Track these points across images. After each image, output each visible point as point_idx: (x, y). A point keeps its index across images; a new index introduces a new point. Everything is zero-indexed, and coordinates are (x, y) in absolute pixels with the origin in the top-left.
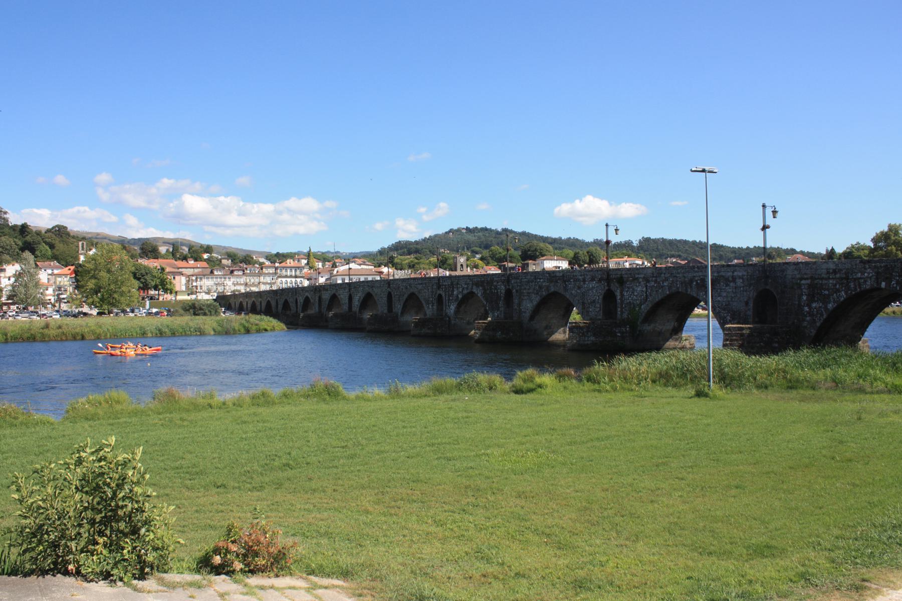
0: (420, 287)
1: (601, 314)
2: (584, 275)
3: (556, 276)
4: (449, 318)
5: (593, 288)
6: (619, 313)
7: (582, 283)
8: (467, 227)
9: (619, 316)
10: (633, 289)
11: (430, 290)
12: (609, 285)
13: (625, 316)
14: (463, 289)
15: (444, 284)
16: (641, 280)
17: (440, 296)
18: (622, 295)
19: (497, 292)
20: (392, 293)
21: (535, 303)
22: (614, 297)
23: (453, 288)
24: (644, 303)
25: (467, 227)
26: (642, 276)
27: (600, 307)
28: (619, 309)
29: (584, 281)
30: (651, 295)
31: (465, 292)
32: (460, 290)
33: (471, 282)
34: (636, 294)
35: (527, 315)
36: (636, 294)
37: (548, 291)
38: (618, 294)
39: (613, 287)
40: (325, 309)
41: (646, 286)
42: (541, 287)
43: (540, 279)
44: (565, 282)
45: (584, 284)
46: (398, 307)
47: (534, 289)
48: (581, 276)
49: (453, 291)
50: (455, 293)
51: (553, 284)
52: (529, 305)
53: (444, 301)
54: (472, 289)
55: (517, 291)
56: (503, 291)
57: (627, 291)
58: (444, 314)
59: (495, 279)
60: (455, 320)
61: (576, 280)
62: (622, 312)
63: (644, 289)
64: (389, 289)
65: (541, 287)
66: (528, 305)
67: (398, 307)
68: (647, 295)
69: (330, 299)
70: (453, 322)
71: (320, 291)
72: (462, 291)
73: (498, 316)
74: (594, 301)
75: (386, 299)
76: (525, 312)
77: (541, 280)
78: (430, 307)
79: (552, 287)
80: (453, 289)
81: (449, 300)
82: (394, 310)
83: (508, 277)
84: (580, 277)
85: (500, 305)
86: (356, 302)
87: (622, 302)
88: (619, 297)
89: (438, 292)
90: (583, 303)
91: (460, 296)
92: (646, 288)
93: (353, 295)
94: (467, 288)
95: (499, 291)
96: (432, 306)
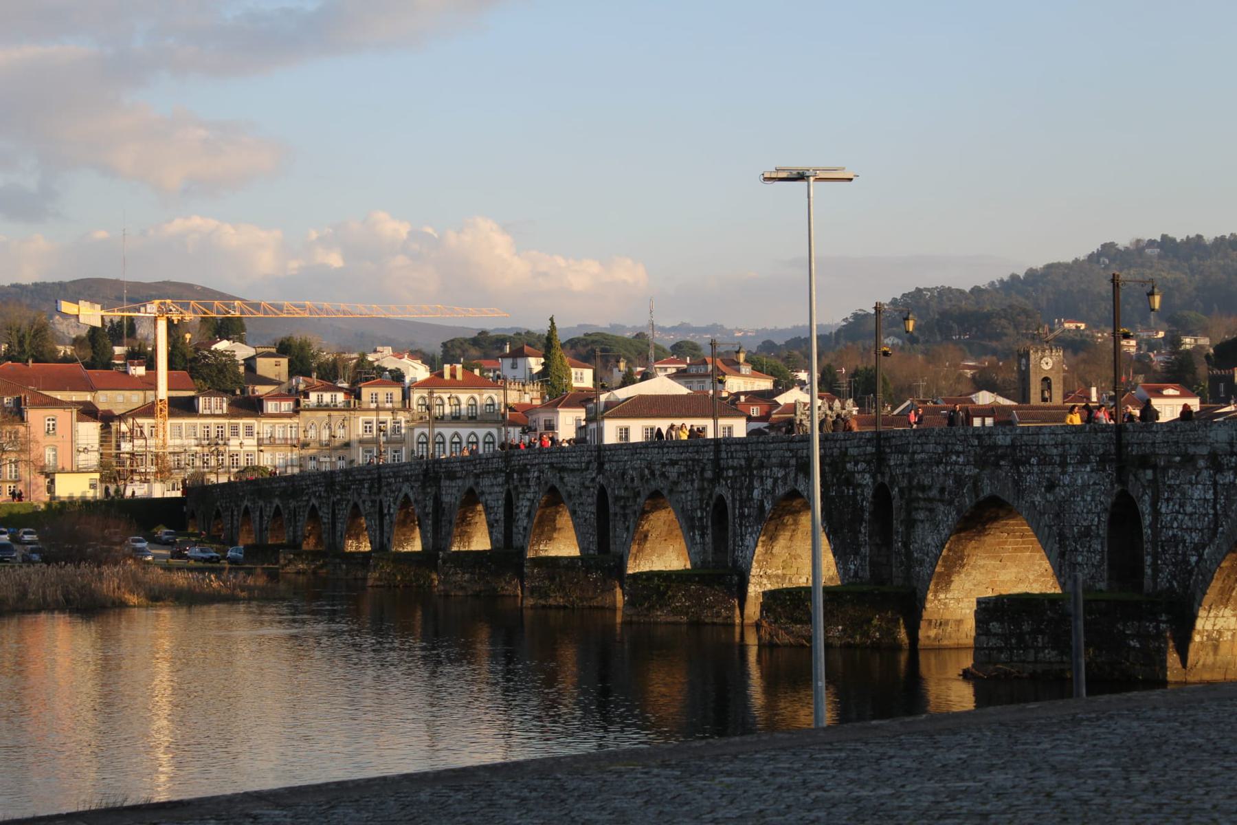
1: (1106, 575)
2: (1063, 444)
3: (995, 447)
5: (1085, 486)
6: (1149, 571)
7: (1059, 470)
8: (1164, 237)
9: (1147, 583)
10: (1184, 494)
12: (1121, 479)
13: (1163, 584)
14: (776, 480)
16: (1201, 463)
17: (721, 499)
18: (1156, 513)
19: (855, 494)
20: (609, 491)
22: (1136, 517)
23: (752, 476)
24: (1211, 540)
25: (1164, 237)
26: (1205, 451)
27: (1103, 551)
28: (1148, 560)
29: (1063, 464)
30: (1227, 516)
33: (793, 462)
34: (1189, 509)
36: (1189, 509)
37: (977, 496)
38: (1145, 507)
39: (1134, 490)
41: (1215, 484)
42: (959, 481)
43: (958, 454)
44: (1016, 463)
45: (1064, 473)
47: (942, 490)
48: (1056, 446)
49: (751, 489)
50: (756, 493)
51: (987, 471)
52: (929, 540)
53: (730, 517)
54: (796, 481)
55: (901, 491)
56: (869, 492)
57: (1168, 500)
58: (730, 565)
59: (852, 451)
61: (1044, 461)
62: (1156, 570)
63: (1210, 495)
64: (600, 479)
65: (959, 481)
68: (1216, 514)
71: (437, 480)
72: (774, 489)
73: (856, 573)
74: (1087, 533)
77: (961, 460)
78: (698, 537)
79: (986, 481)
80: (751, 482)
81: (742, 515)
82: (612, 547)
84: (1055, 451)
85: (861, 538)
87: (1156, 533)
88: (1147, 520)
90: (1062, 537)
92: (1215, 493)
95: (859, 491)
96: (702, 536)
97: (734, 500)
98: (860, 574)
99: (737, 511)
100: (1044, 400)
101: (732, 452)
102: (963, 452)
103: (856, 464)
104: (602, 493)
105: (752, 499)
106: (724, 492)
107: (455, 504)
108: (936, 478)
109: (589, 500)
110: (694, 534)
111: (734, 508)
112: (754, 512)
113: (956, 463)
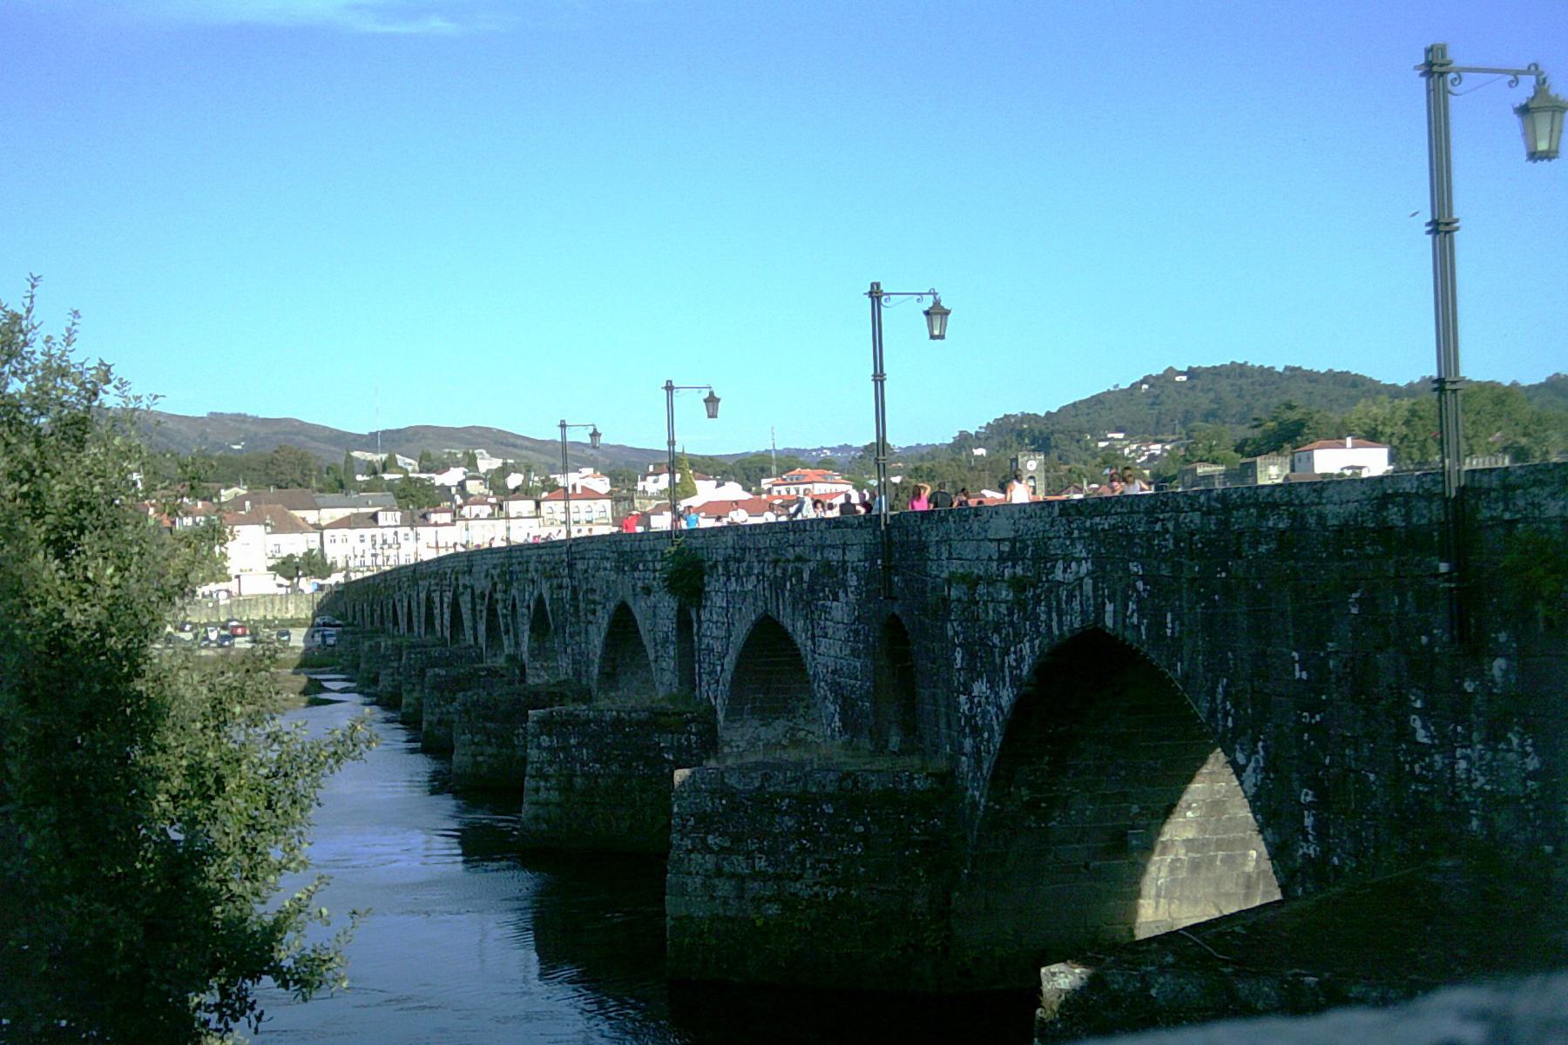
25: (1190, 368)
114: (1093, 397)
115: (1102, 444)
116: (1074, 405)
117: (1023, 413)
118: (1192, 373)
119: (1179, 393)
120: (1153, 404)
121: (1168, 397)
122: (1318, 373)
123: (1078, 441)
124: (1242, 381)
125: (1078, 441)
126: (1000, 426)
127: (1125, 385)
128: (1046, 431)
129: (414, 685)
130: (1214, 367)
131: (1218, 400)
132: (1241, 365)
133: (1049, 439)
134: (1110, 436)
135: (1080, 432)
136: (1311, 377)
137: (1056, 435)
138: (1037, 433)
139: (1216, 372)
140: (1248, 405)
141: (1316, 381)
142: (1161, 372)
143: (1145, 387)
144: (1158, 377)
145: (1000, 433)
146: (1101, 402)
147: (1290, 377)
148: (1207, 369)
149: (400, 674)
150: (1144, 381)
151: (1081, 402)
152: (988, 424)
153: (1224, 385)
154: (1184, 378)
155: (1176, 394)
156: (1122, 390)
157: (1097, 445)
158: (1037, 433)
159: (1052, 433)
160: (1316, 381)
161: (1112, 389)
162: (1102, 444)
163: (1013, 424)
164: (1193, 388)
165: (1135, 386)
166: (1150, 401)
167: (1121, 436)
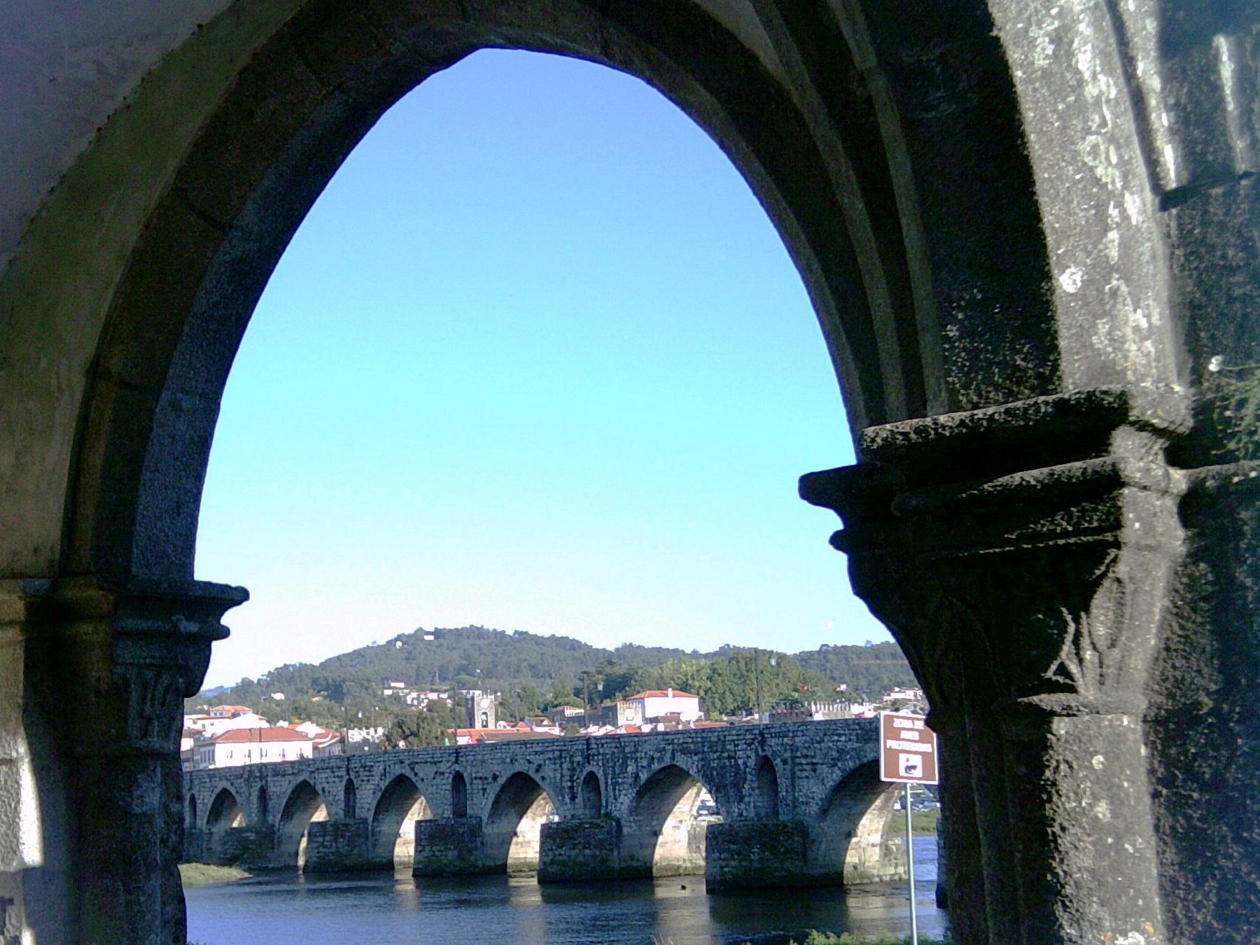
0: (537, 760)
4: (618, 822)
8: (436, 629)
11: (565, 766)
15: (601, 751)
17: (592, 775)
19: (737, 764)
20: (465, 775)
21: (830, 784)
23: (625, 759)
25: (436, 629)
31: (656, 766)
32: (645, 763)
35: (814, 808)
40: (279, 816)
43: (840, 735)
46: (481, 805)
47: (826, 755)
49: (624, 765)
50: (629, 769)
52: (814, 789)
54: (673, 758)
55: (785, 762)
56: (752, 762)
60: (630, 827)
64: (457, 767)
66: (814, 790)
67: (481, 805)
69: (293, 792)
70: (625, 831)
73: (741, 815)
75: (449, 787)
76: (807, 803)
77: (843, 738)
78: (567, 800)
81: (615, 784)
82: (469, 811)
83: (762, 734)
86: (367, 798)
89: (588, 768)
91: (644, 776)
93: (356, 782)
94: (661, 760)
95: (740, 762)
96: (573, 798)
97: (606, 774)
98: (745, 814)
99: (609, 781)
100: (484, 726)
101: (603, 744)
102: (845, 735)
103: (736, 746)
104: (458, 777)
105: (626, 772)
106: (594, 769)
107: (284, 792)
108: (818, 751)
109: (444, 782)
110: (564, 797)
111: (606, 778)
112: (630, 781)
113: (838, 741)
114: (355, 651)
115: (388, 692)
116: (339, 658)
117: (301, 664)
118: (438, 633)
119: (428, 650)
120: (407, 659)
121: (420, 654)
122: (542, 637)
123: (367, 689)
124: (480, 642)
125: (367, 689)
126: (280, 674)
127: (382, 642)
128: (339, 679)
129: (424, 846)
130: (457, 629)
131: (467, 657)
132: (478, 628)
133: (341, 686)
134: (393, 685)
135: (369, 681)
136: (537, 640)
137: (348, 683)
138: (330, 681)
139: (458, 633)
140: (493, 662)
141: (542, 644)
142: (412, 632)
143: (399, 644)
144: (410, 636)
145: (279, 681)
146: (362, 656)
147: (519, 641)
148: (450, 630)
149: (325, 847)
150: (397, 639)
151: (344, 655)
152: (270, 672)
153: (466, 644)
154: (431, 638)
155: (426, 651)
156: (378, 646)
157: (383, 693)
158: (330, 681)
159: (344, 681)
160: (542, 644)
161: (371, 645)
162: (388, 692)
163: (292, 673)
164: (441, 646)
165: (391, 643)
166: (404, 656)
167: (401, 685)
